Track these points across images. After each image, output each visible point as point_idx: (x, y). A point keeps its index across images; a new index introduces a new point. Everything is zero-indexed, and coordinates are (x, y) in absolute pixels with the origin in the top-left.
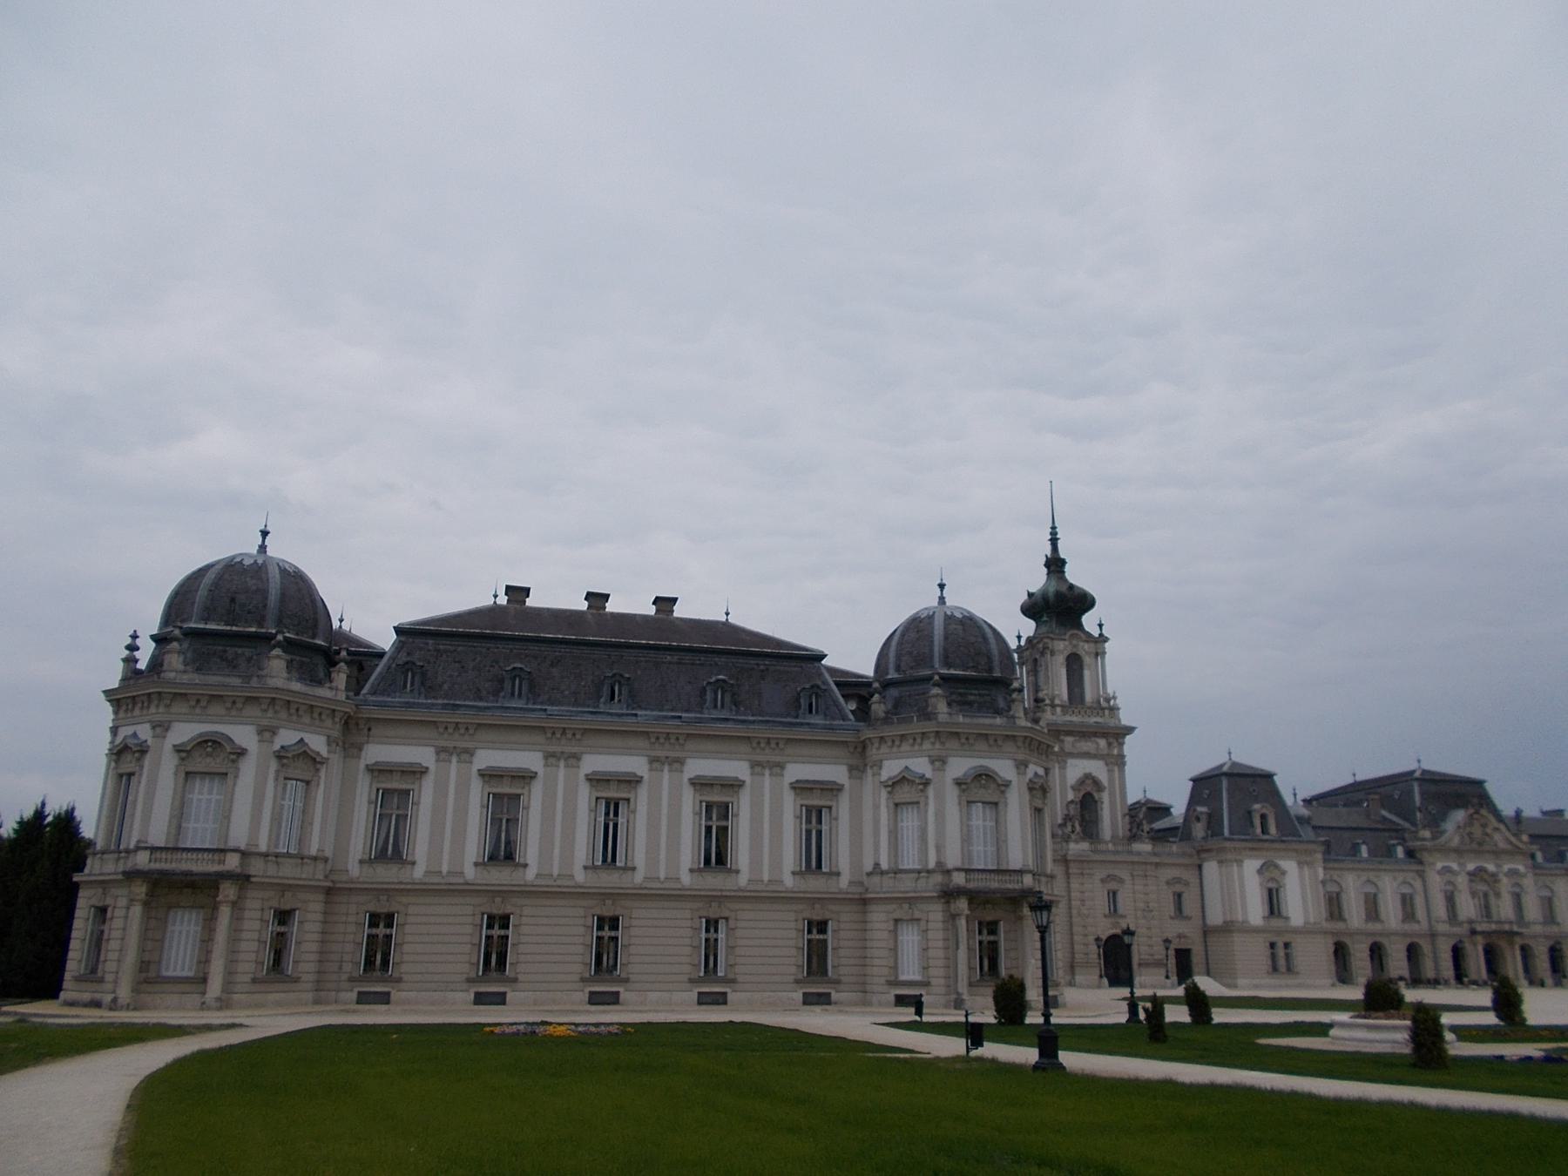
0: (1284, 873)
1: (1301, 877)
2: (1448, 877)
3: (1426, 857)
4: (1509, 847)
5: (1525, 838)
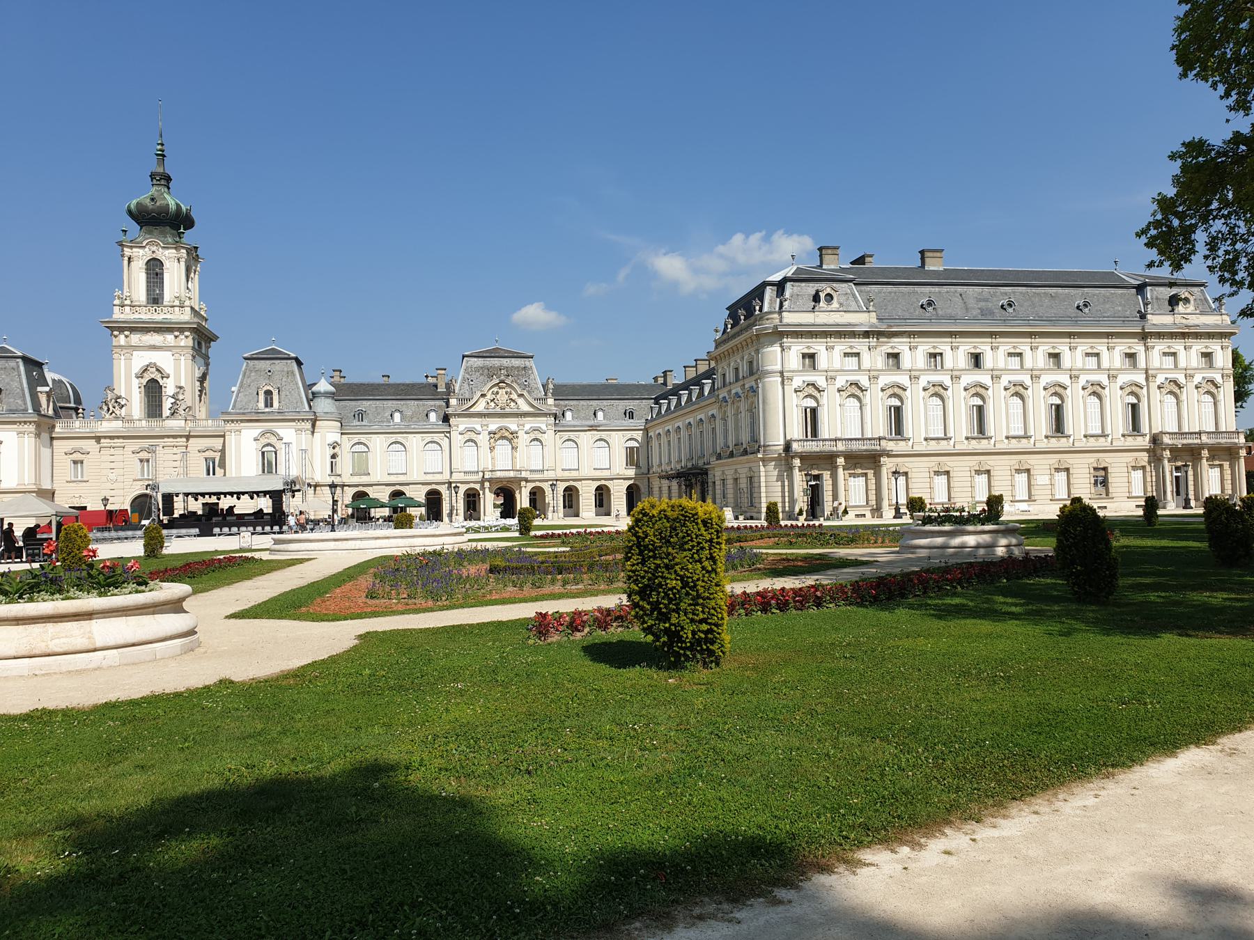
3: (452, 421)
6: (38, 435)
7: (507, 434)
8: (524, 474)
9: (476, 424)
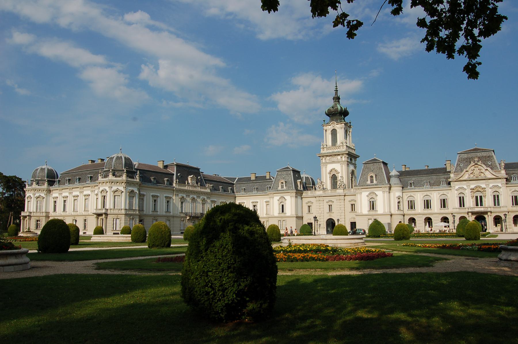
1: (384, 197)
4: (494, 177)
6: (296, 197)
7: (480, 190)
8: (489, 210)
9: (464, 185)
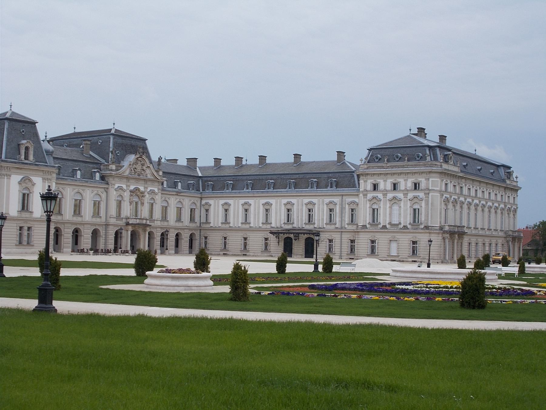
0: (34, 184)
2: (121, 192)
3: (111, 180)
5: (161, 173)
